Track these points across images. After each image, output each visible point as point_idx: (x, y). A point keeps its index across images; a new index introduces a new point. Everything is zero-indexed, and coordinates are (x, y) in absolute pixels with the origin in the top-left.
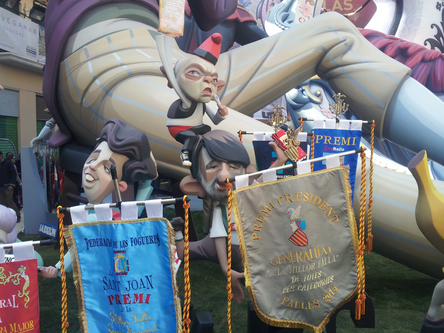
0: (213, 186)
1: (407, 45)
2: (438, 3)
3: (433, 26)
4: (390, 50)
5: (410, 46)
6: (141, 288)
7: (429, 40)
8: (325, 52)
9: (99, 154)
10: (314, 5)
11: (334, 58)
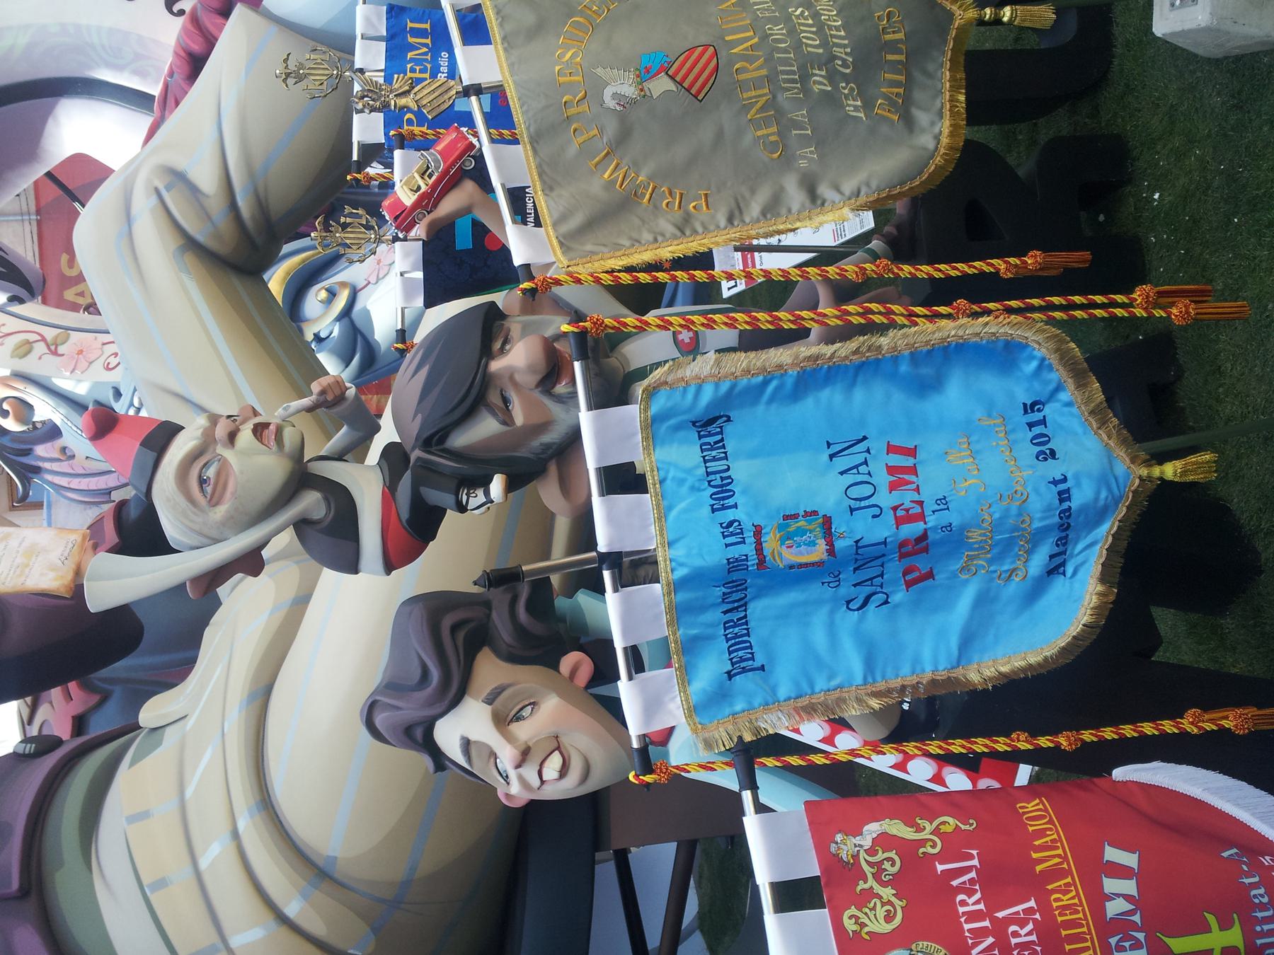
0: (564, 400)
1: (183, 58)
5: (185, 51)
6: (869, 471)
8: (190, 244)
9: (475, 742)
10: (69, 331)
11: (209, 217)
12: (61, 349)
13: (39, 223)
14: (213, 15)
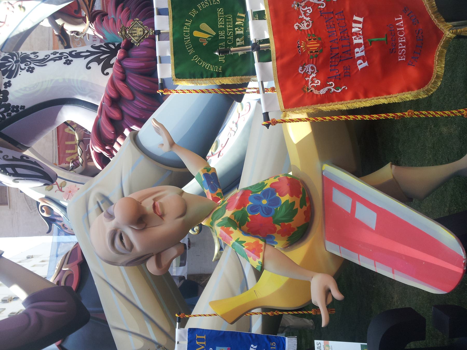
1: (108, 99)
2: (65, 63)
4: (113, 114)
5: (108, 96)
7: (103, 70)
10: (66, 181)
12: (63, 189)
14: (119, 81)
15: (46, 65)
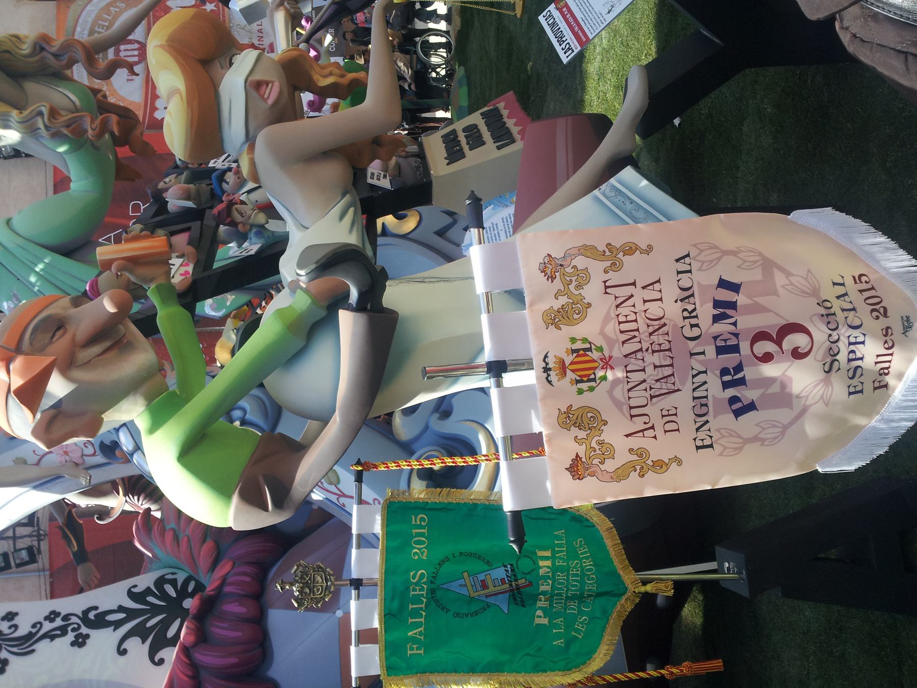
3: (121, 650)
7: (152, 657)
13: (52, 584)
15: (33, 651)
